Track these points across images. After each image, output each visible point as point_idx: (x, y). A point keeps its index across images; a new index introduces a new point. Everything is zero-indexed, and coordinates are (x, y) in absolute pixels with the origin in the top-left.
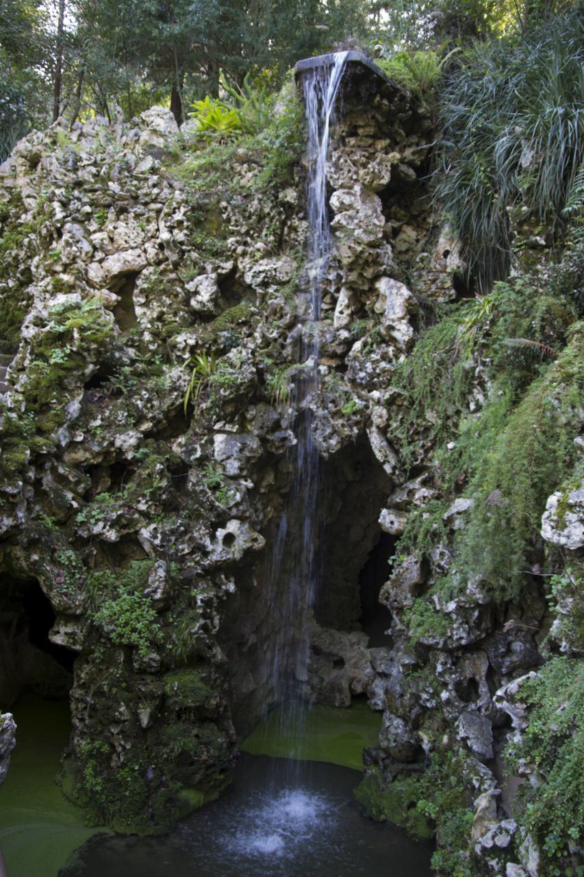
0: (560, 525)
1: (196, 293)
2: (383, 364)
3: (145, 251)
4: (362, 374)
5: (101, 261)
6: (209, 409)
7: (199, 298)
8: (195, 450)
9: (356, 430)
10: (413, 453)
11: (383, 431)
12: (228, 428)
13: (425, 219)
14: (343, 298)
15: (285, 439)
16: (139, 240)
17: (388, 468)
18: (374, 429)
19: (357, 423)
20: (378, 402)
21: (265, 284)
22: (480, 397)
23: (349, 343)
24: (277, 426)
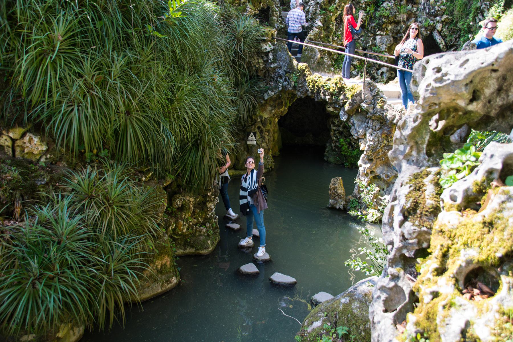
2: (442, 7)
4: (432, 11)
6: (375, 26)
8: (369, 42)
11: (440, 32)
12: (382, 33)
17: (441, 46)
18: (436, 31)
20: (438, 22)
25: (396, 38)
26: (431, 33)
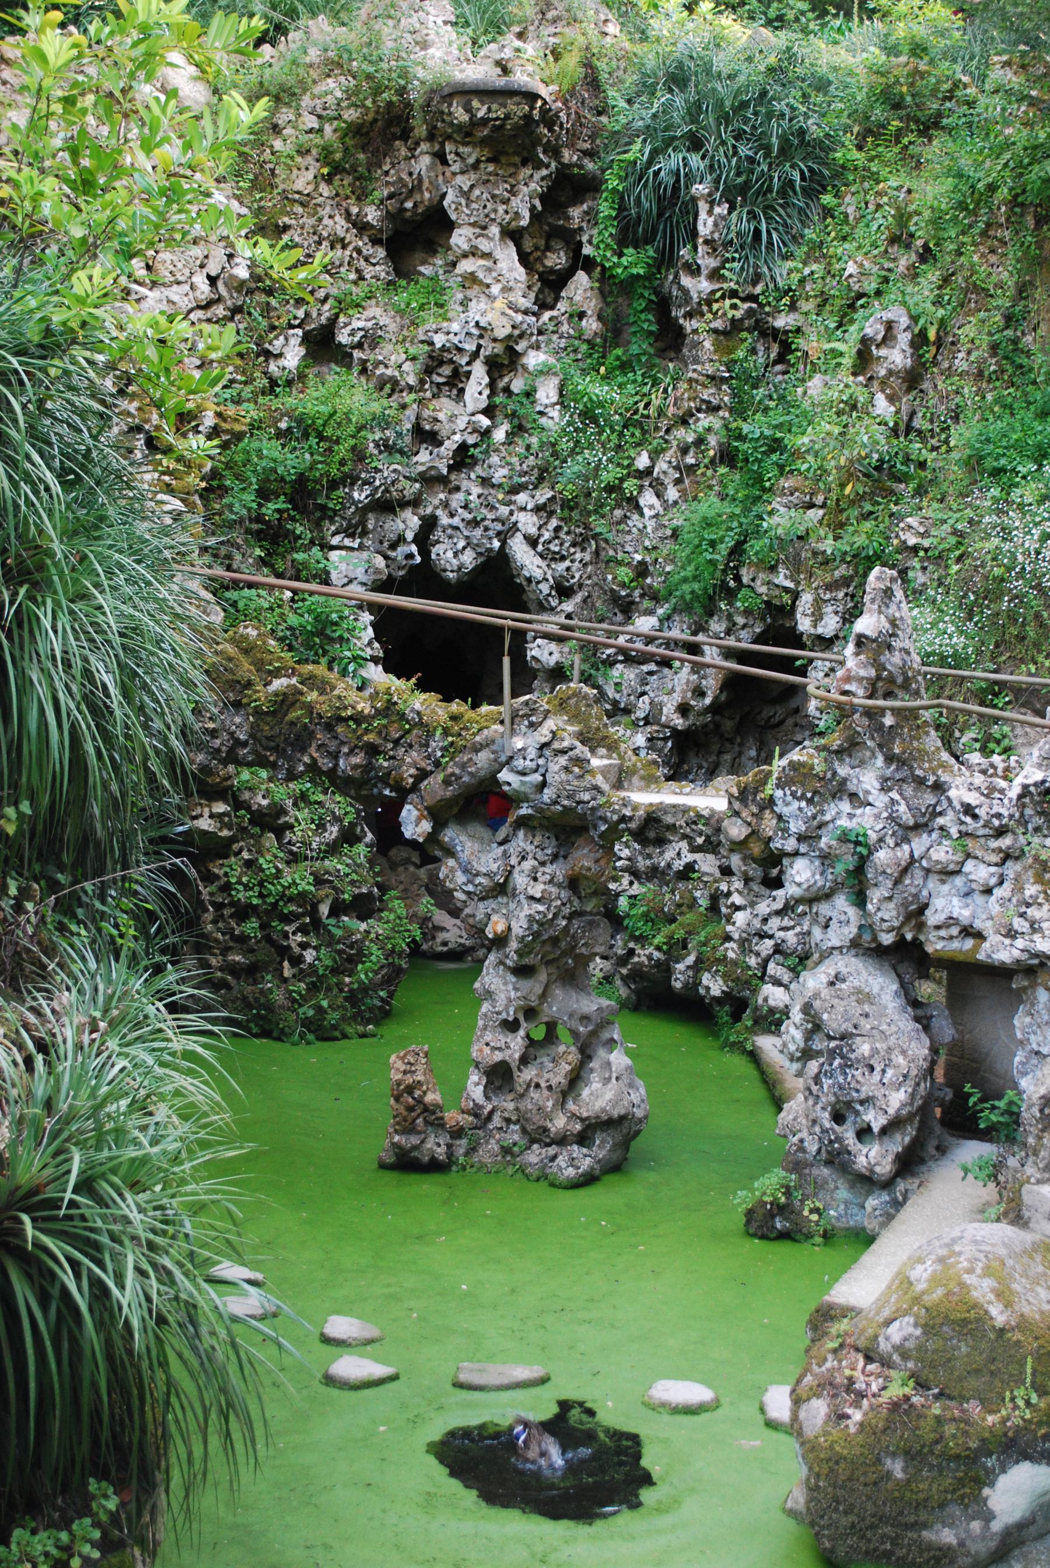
0: (817, 617)
1: (280, 355)
3: (193, 287)
5: (138, 301)
7: (282, 362)
9: (496, 544)
10: (568, 569)
11: (532, 542)
12: (347, 542)
13: (539, 259)
14: (479, 372)
15: (410, 556)
16: (187, 272)
19: (499, 534)
21: (360, 346)
22: (654, 500)
23: (486, 433)
24: (401, 539)
25: (394, 560)
26: (504, 543)
